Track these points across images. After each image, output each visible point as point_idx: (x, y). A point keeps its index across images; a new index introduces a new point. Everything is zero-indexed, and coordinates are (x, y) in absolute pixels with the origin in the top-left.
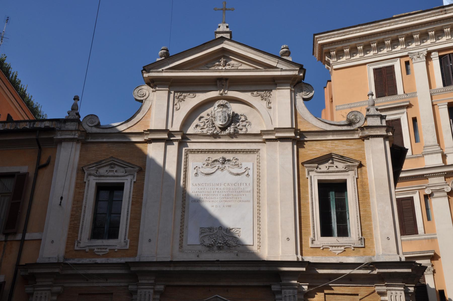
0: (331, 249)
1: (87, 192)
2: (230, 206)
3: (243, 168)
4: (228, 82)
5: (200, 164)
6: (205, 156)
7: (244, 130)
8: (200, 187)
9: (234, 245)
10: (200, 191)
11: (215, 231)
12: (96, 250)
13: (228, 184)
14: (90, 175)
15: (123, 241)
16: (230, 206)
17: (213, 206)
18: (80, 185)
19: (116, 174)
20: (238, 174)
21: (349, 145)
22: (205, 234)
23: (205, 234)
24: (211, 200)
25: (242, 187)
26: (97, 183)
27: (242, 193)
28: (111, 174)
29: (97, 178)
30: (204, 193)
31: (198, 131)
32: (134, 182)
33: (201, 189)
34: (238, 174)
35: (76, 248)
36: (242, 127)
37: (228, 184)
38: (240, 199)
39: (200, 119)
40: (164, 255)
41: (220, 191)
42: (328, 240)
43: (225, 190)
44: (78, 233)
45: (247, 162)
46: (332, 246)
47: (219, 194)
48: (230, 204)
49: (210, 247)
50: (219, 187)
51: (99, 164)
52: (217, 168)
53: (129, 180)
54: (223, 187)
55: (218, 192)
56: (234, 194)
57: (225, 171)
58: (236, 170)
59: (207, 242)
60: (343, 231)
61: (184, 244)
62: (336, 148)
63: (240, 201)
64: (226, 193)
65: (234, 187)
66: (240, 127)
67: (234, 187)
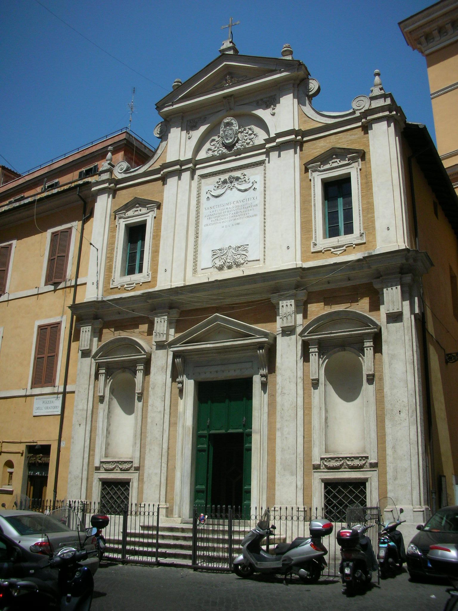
0: (333, 250)
1: (119, 234)
2: (238, 224)
3: (251, 182)
4: (232, 98)
5: (211, 188)
6: (216, 179)
7: (251, 143)
8: (211, 210)
9: (242, 262)
10: (212, 214)
11: (226, 251)
12: (126, 286)
13: (237, 202)
14: (120, 218)
15: (147, 274)
16: (238, 224)
17: (223, 227)
18: (113, 229)
19: (140, 213)
20: (246, 190)
21: (352, 135)
22: (216, 256)
23: (216, 256)
24: (222, 221)
25: (250, 202)
26: (127, 226)
27: (250, 208)
28: (136, 213)
29: (126, 220)
30: (215, 216)
31: (210, 154)
32: (155, 218)
33: (213, 211)
34: (246, 190)
35: (111, 287)
36: (249, 141)
37: (237, 202)
38: (248, 215)
39: (211, 142)
40: (178, 283)
41: (229, 210)
42: (334, 241)
43: (234, 209)
44: (112, 272)
45: (254, 175)
46: (334, 248)
47: (228, 213)
48: (238, 221)
49: (221, 268)
50: (228, 207)
51: (127, 207)
52: (227, 187)
53: (151, 216)
54: (231, 206)
55: (228, 211)
56: (242, 210)
57: (234, 189)
58: (242, 187)
59: (219, 263)
60: (349, 230)
61: (199, 269)
62: (340, 141)
63: (248, 217)
64: (235, 212)
65: (242, 203)
66: (248, 141)
67: (242, 203)
